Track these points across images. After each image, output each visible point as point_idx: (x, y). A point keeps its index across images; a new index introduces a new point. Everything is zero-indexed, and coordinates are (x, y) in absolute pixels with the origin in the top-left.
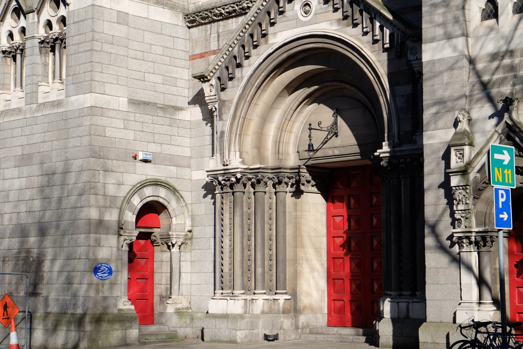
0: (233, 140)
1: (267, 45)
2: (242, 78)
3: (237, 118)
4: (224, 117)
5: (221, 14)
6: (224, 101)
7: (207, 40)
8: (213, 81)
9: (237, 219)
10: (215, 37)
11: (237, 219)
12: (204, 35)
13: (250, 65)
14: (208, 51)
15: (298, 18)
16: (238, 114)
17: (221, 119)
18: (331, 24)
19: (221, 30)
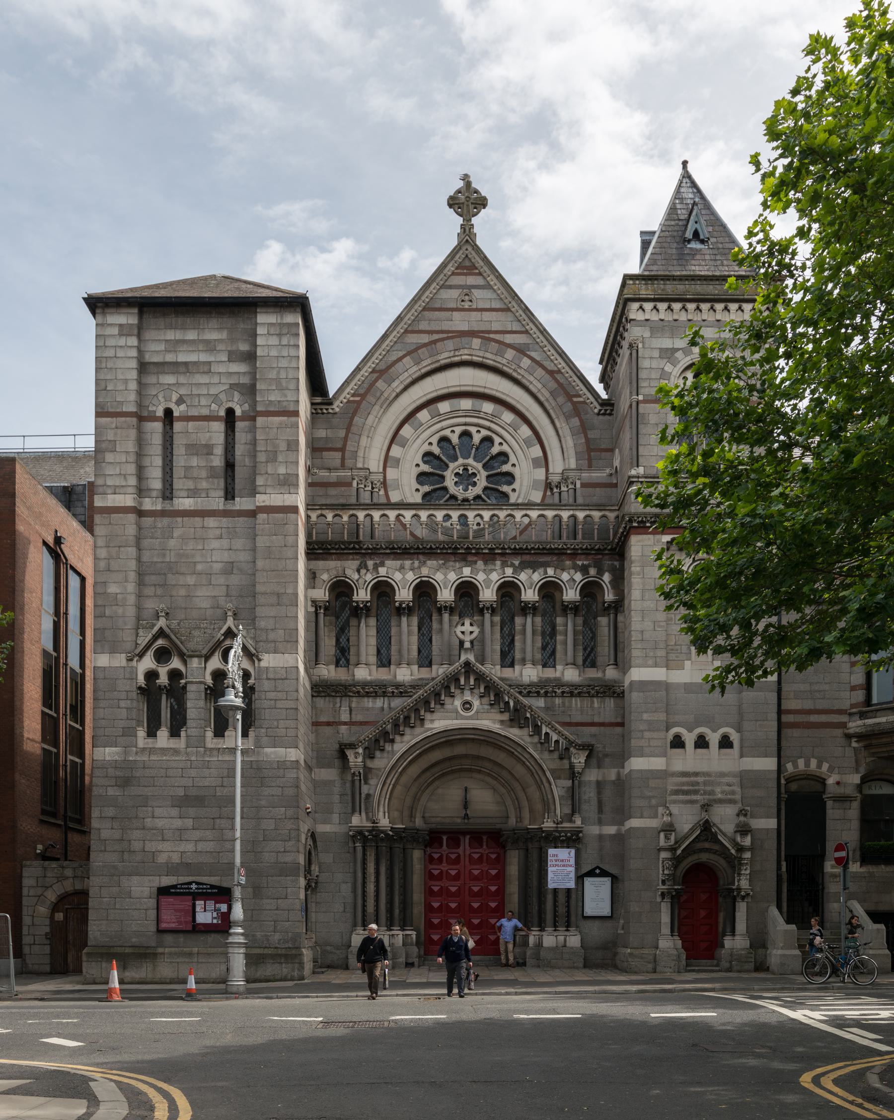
0: (382, 803)
1: (422, 729)
2: (393, 753)
3: (387, 785)
4: (372, 782)
5: (358, 692)
6: (370, 769)
7: (337, 711)
8: (360, 750)
9: (383, 870)
10: (345, 711)
11: (383, 870)
12: (331, 706)
13: (402, 742)
14: (337, 720)
15: (457, 712)
16: (388, 781)
17: (366, 783)
18: (494, 723)
19: (354, 705)
